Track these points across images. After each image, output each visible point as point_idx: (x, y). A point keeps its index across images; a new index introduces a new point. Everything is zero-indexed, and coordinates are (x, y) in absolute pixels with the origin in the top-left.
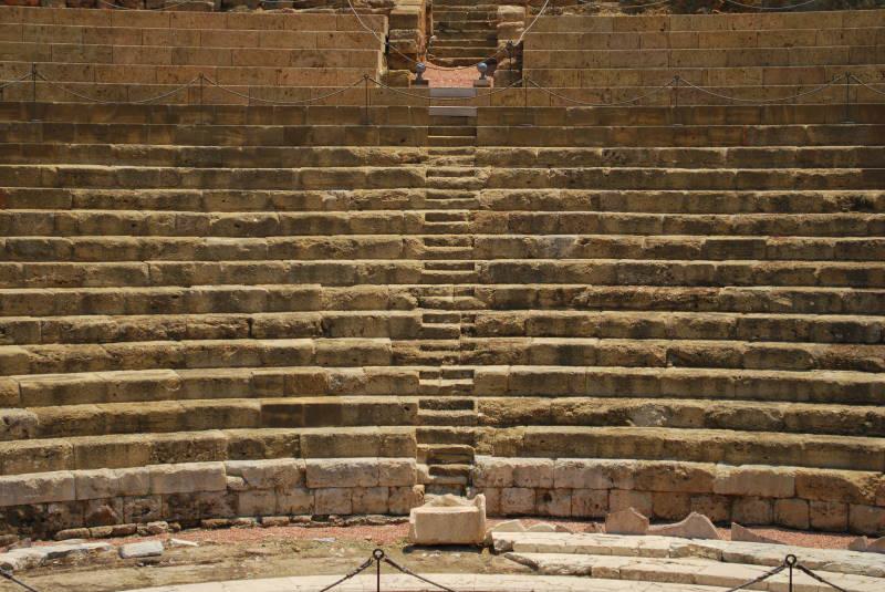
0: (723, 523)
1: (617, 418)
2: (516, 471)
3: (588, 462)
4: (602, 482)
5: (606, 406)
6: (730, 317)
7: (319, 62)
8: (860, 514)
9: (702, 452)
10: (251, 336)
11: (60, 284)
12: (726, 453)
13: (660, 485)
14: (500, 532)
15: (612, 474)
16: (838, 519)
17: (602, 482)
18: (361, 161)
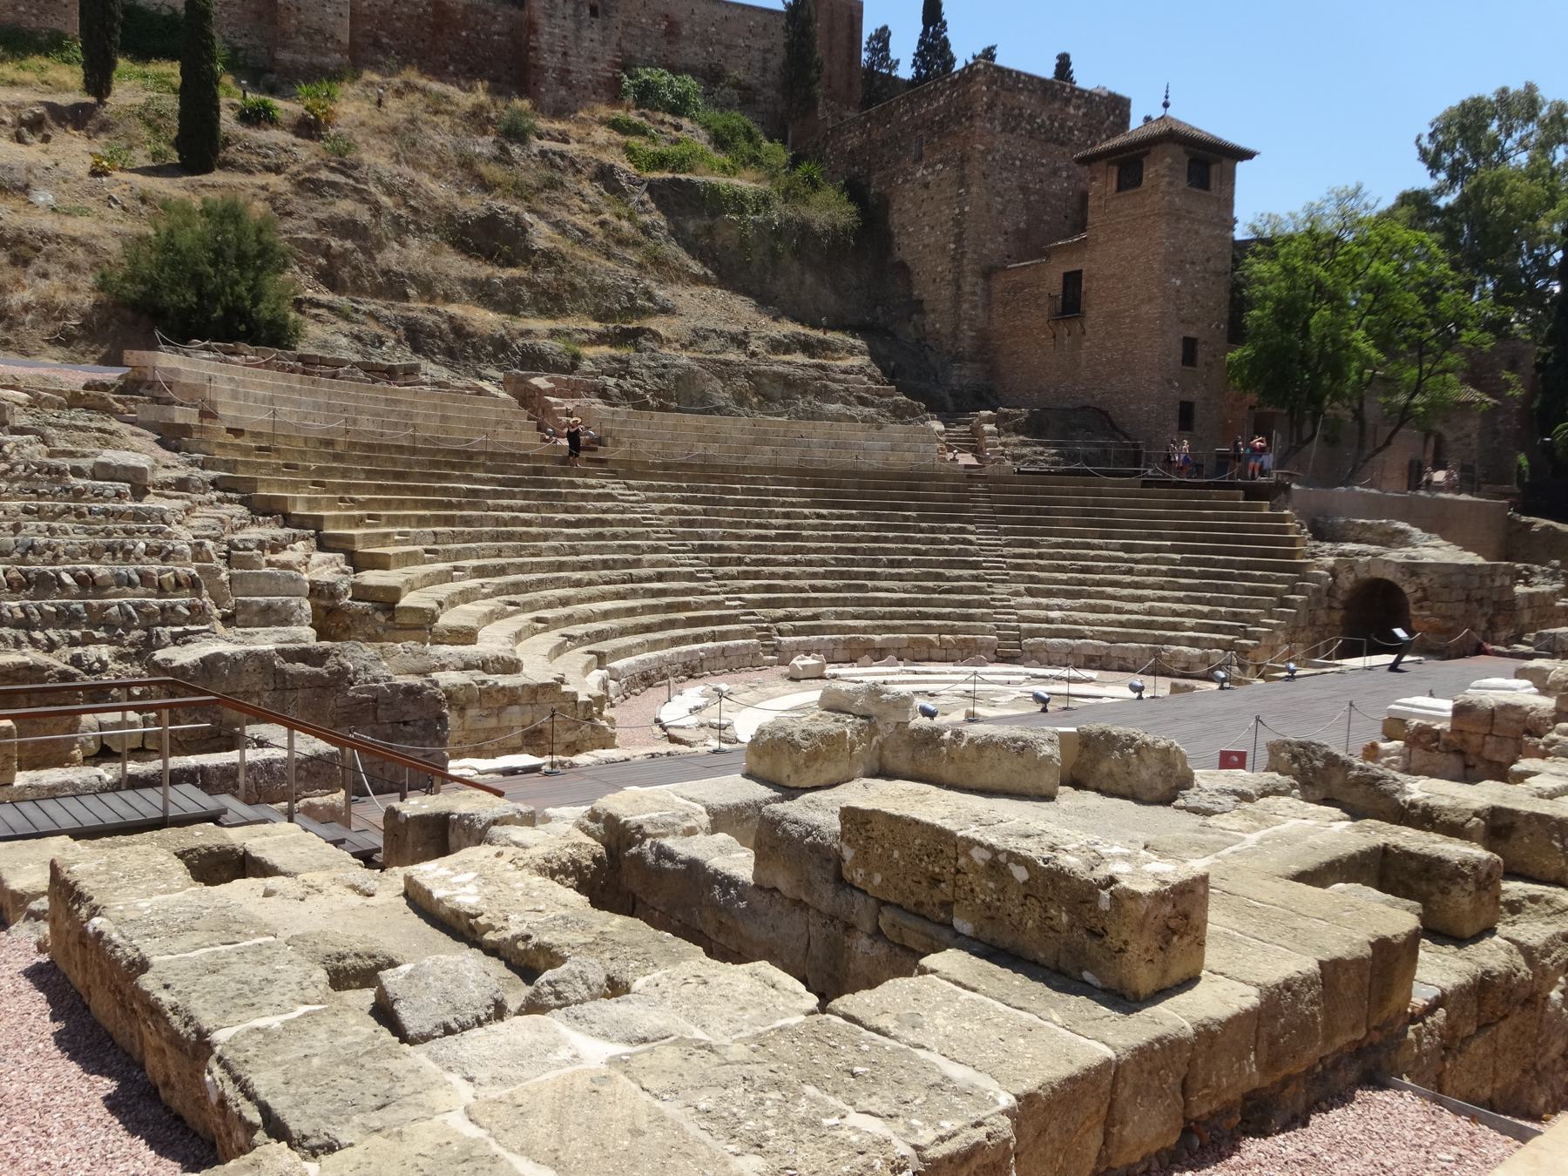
0: (900, 659)
1: (815, 617)
2: (799, 643)
3: (826, 637)
4: (831, 646)
5: (809, 611)
6: (822, 569)
7: (509, 426)
8: (935, 653)
9: (865, 630)
10: (632, 582)
11: (533, 555)
12: (875, 629)
13: (854, 646)
14: (830, 670)
15: (835, 642)
16: (926, 655)
17: (831, 646)
18: (578, 486)
